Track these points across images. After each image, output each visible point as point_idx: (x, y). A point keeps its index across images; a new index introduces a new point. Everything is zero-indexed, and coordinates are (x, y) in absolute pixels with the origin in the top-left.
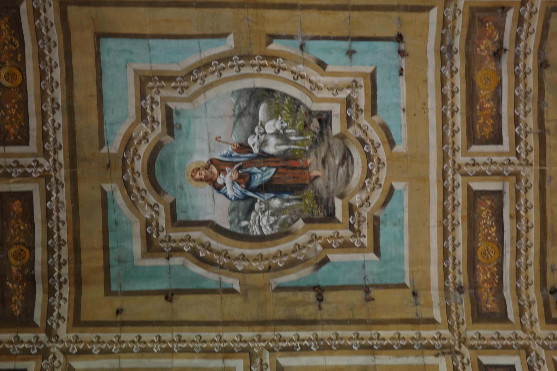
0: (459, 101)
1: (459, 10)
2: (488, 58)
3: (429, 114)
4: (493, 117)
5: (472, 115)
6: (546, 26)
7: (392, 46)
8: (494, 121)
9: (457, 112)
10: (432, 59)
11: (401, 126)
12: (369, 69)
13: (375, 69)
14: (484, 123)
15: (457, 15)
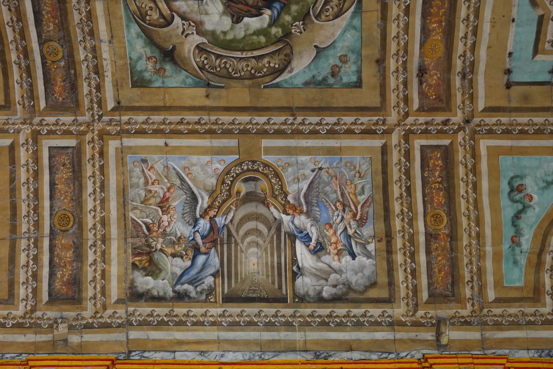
0: (461, 29)
1: (460, 109)
2: (431, 67)
3: (490, 17)
4: (431, 14)
5: (450, 17)
6: (383, 95)
7: (516, 77)
8: (430, 11)
9: (464, 19)
10: (482, 67)
11: (519, 5)
12: (539, 57)
13: (533, 59)
14: (439, 9)
15: (462, 105)
